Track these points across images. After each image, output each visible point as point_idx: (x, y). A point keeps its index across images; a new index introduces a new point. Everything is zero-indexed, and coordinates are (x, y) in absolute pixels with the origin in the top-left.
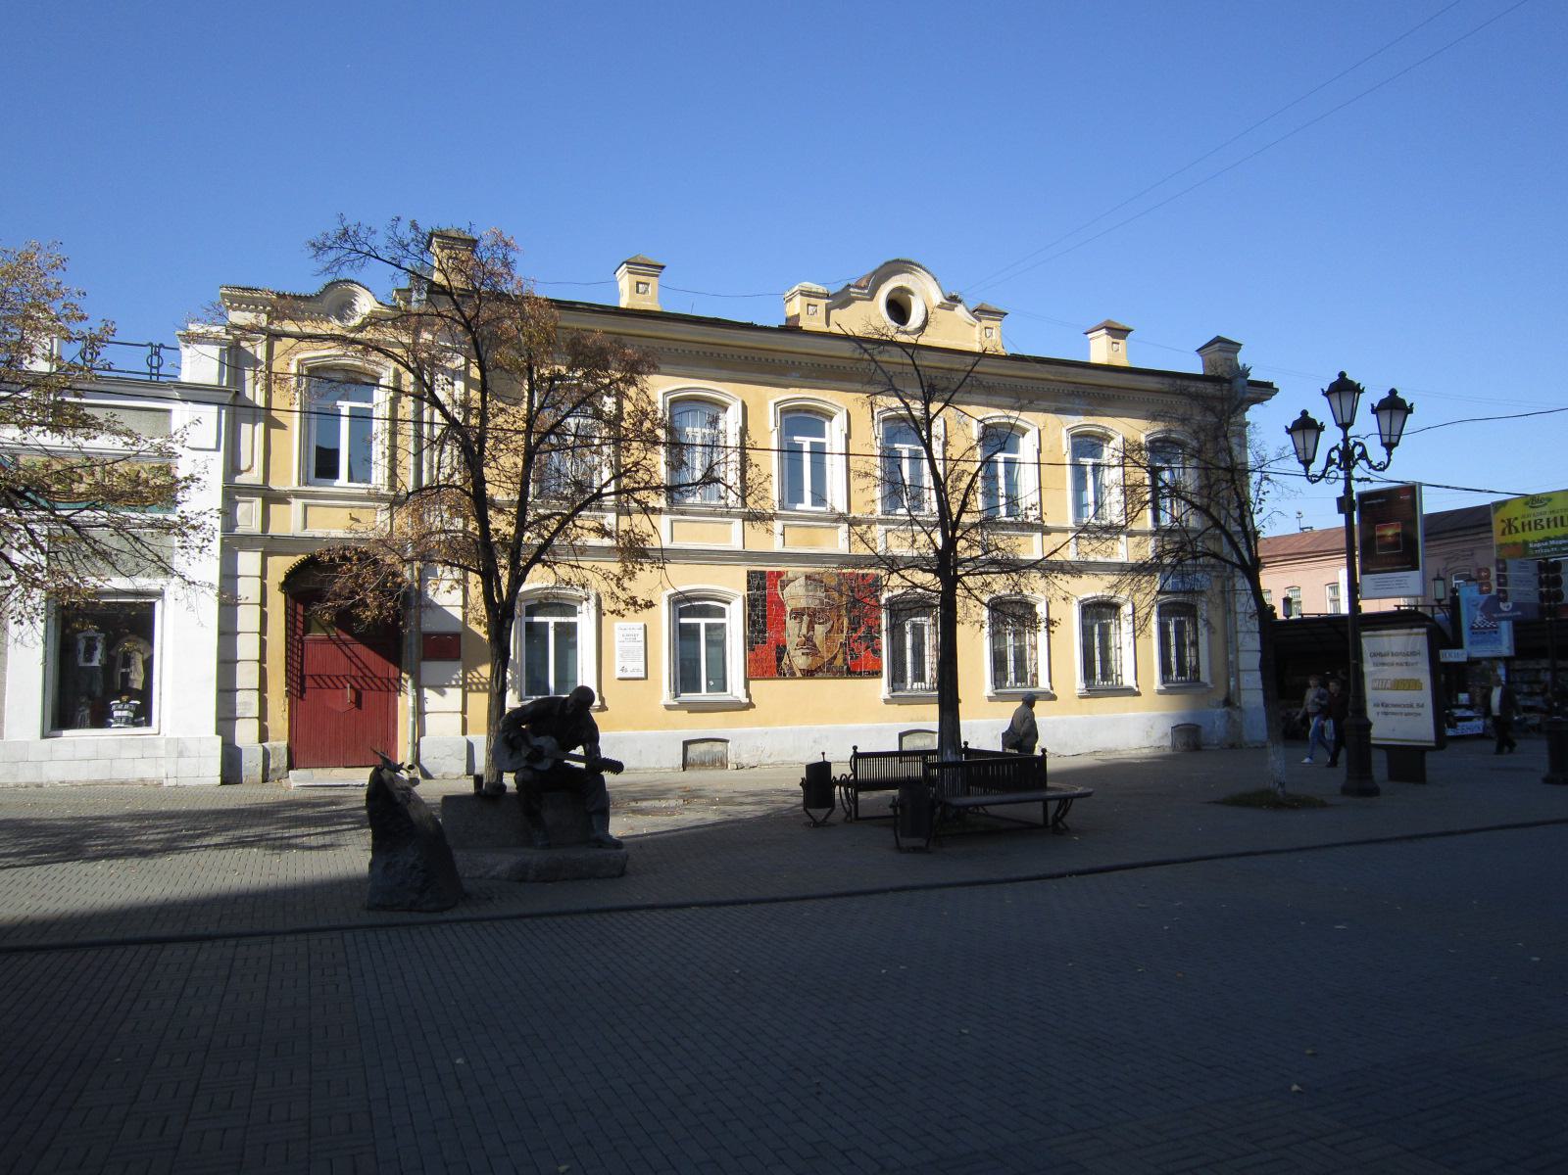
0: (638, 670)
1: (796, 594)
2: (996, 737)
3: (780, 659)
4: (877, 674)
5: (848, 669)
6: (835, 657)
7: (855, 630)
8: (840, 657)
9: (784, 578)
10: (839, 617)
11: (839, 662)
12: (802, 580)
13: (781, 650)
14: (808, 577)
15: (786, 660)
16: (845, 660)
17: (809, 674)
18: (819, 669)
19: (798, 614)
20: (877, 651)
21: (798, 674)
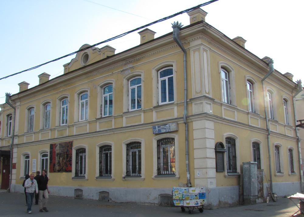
0: (34, 170)
1: (58, 150)
2: (97, 193)
3: (54, 167)
4: (71, 171)
5: (66, 170)
6: (63, 167)
7: (67, 158)
8: (64, 167)
9: (56, 145)
10: (65, 155)
11: (64, 168)
12: (59, 145)
13: (54, 165)
14: (60, 144)
15: (55, 168)
16: (65, 167)
17: (59, 171)
18: (60, 170)
19: (58, 154)
20: (71, 165)
21: (57, 171)
